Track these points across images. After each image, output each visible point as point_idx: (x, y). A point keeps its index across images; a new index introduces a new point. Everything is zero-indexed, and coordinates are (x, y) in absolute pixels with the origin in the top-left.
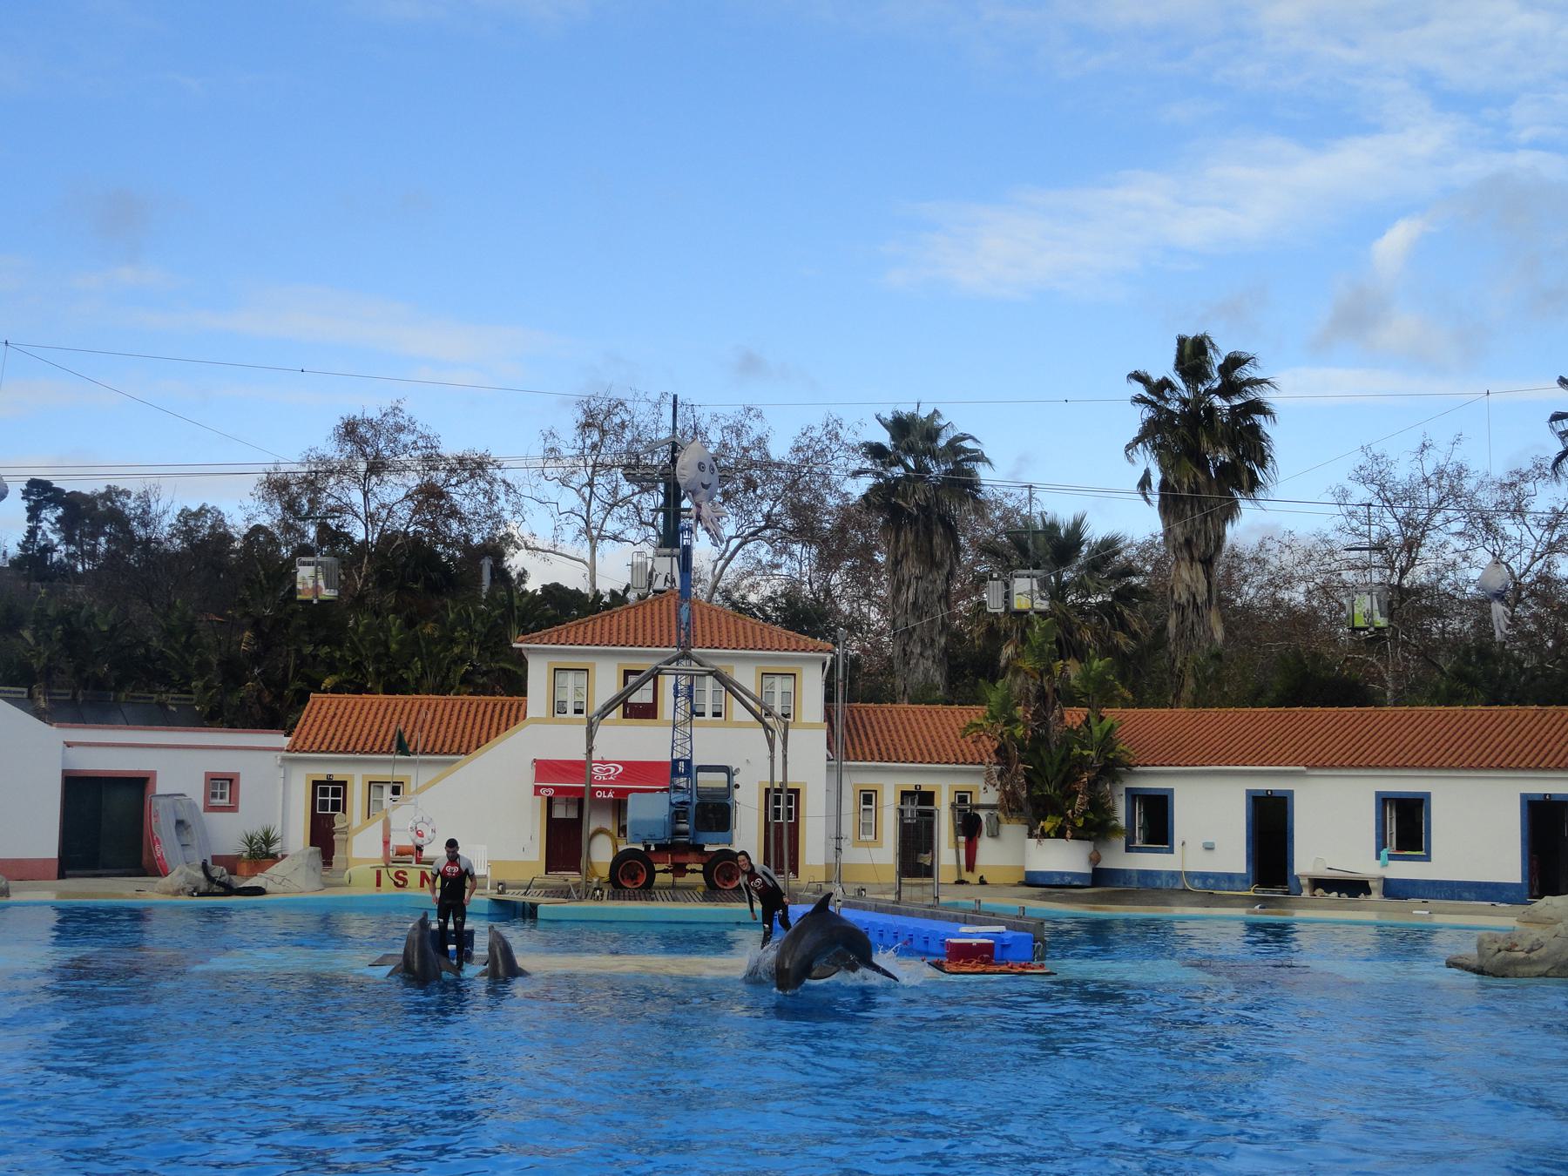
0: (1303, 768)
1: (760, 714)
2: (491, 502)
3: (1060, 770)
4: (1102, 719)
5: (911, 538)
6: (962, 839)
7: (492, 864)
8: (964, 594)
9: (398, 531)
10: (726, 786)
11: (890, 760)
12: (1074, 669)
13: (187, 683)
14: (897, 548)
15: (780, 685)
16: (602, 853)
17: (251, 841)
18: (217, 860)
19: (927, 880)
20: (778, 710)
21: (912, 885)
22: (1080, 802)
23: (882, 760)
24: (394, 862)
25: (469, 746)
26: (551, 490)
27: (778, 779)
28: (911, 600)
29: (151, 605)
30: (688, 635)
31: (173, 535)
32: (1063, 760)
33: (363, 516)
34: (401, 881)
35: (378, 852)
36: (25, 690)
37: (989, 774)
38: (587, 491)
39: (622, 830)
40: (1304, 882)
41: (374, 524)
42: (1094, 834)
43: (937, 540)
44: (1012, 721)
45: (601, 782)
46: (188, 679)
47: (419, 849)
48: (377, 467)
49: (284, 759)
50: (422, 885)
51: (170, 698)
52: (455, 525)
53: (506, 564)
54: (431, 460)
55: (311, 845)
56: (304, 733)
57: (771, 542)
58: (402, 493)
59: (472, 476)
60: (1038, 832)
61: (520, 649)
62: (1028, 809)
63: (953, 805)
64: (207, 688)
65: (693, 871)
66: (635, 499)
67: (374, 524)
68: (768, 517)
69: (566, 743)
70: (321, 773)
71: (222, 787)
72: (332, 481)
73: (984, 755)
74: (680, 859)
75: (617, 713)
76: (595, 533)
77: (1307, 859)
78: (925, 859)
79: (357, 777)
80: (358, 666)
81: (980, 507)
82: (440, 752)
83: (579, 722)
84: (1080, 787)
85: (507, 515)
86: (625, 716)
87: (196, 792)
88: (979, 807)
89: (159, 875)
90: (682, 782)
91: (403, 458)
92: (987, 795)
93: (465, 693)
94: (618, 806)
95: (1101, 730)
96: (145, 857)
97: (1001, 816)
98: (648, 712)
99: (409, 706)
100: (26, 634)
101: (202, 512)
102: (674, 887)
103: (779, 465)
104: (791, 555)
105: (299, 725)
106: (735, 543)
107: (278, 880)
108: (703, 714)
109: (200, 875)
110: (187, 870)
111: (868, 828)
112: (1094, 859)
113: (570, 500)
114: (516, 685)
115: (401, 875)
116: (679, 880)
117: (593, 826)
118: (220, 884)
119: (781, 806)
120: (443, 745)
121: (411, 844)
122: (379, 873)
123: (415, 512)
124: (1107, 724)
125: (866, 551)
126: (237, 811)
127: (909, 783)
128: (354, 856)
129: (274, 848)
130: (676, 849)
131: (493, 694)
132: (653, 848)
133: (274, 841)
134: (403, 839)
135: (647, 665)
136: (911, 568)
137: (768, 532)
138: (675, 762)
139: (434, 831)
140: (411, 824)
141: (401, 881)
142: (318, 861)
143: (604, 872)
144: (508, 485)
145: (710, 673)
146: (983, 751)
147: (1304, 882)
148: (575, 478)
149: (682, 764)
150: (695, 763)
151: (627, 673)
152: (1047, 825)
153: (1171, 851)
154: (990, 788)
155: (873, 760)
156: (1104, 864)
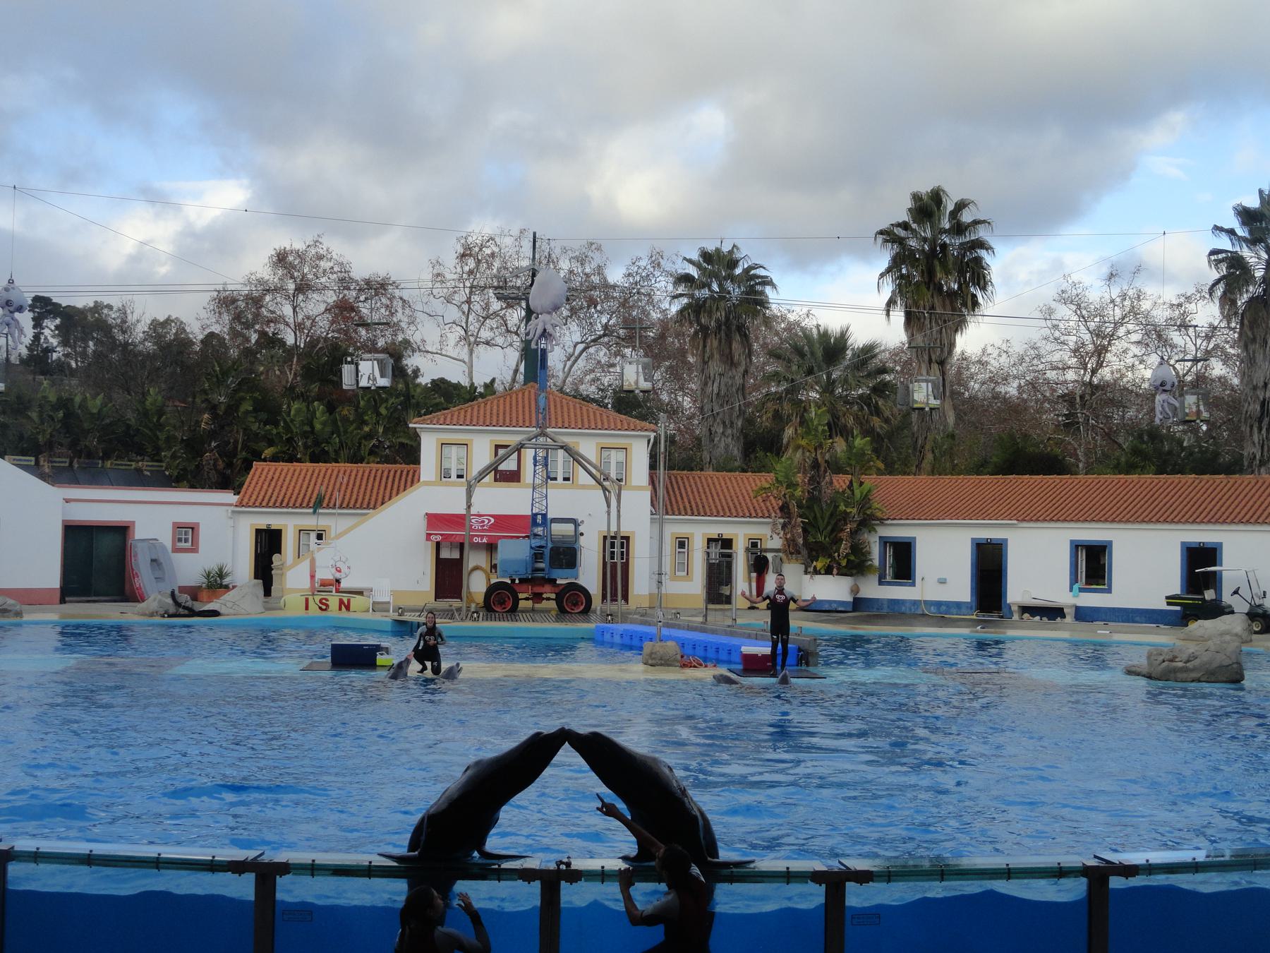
0: (1015, 522)
1: (601, 480)
2: (392, 314)
3: (828, 523)
4: (861, 484)
5: (715, 343)
6: (754, 575)
7: (394, 593)
8: (756, 388)
9: (320, 337)
10: (573, 534)
11: (699, 514)
12: (840, 445)
13: (158, 454)
14: (704, 351)
15: (615, 457)
16: (477, 585)
17: (208, 576)
18: (183, 589)
19: (727, 606)
20: (613, 475)
21: (716, 610)
22: (844, 548)
23: (693, 514)
24: (319, 591)
25: (376, 503)
26: (437, 306)
27: (614, 528)
28: (716, 391)
29: (129, 394)
30: (544, 419)
31: (145, 340)
32: (832, 515)
33: (292, 326)
34: (324, 606)
35: (306, 584)
36: (33, 458)
37: (775, 524)
38: (465, 307)
39: (494, 567)
41: (301, 330)
42: (854, 571)
43: (735, 345)
44: (791, 485)
45: (478, 531)
46: (158, 450)
47: (338, 581)
48: (303, 287)
49: (233, 512)
50: (340, 609)
51: (145, 465)
52: (363, 332)
53: (405, 362)
54: (345, 283)
55: (256, 577)
56: (249, 492)
57: (607, 345)
58: (322, 308)
59: (376, 295)
60: (811, 569)
61: (415, 428)
62: (805, 552)
63: (747, 549)
64: (174, 457)
65: (548, 599)
66: (503, 312)
67: (301, 330)
68: (606, 327)
69: (450, 501)
70: (263, 522)
71: (187, 534)
72: (268, 298)
73: (772, 511)
74: (538, 590)
75: (489, 478)
76: (472, 339)
77: (1017, 591)
78: (725, 590)
79: (289, 524)
80: (290, 441)
81: (768, 321)
82: (354, 507)
83: (461, 485)
84: (844, 535)
85: (403, 325)
86: (496, 480)
87: (166, 539)
88: (767, 550)
89: (138, 601)
90: (539, 530)
91: (323, 280)
92: (776, 542)
93: (373, 462)
94: (491, 548)
95: (862, 493)
96: (127, 587)
97: (784, 557)
98: (513, 477)
99: (329, 471)
100: (34, 415)
101: (168, 321)
102: (533, 610)
103: (614, 287)
104: (623, 356)
105: (245, 486)
106: (581, 347)
107: (229, 605)
108: (555, 479)
109: (170, 601)
110: (159, 597)
112: (855, 590)
113: (453, 313)
114: (411, 454)
115: (324, 601)
116: (537, 606)
117: (471, 566)
118: (185, 608)
119: (615, 550)
120: (356, 502)
121: (331, 577)
122: (307, 600)
123: (332, 322)
124: (866, 486)
125: (682, 353)
126: (197, 552)
127: (714, 531)
128: (288, 587)
129: (226, 581)
130: (535, 581)
131: (395, 462)
132: (517, 581)
133: (227, 575)
134: (325, 574)
135: (512, 440)
136: (715, 367)
137: (606, 339)
138: (535, 515)
139: (349, 568)
140: (332, 562)
141: (324, 606)
142: (261, 591)
143: (480, 599)
144: (404, 301)
145: (562, 447)
146: (770, 508)
147: (1015, 608)
148: (456, 297)
149: (539, 517)
150: (550, 516)
151: (497, 447)
152: (819, 564)
153: (913, 585)
154: (775, 536)
155: (686, 514)
156: (859, 596)
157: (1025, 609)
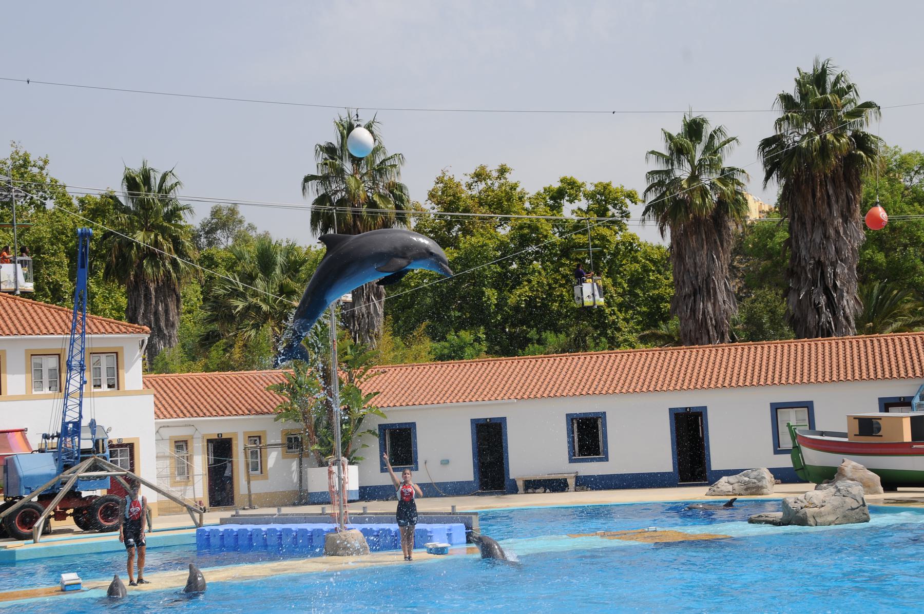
40: (520, 484)
111: (184, 471)
147: (520, 484)
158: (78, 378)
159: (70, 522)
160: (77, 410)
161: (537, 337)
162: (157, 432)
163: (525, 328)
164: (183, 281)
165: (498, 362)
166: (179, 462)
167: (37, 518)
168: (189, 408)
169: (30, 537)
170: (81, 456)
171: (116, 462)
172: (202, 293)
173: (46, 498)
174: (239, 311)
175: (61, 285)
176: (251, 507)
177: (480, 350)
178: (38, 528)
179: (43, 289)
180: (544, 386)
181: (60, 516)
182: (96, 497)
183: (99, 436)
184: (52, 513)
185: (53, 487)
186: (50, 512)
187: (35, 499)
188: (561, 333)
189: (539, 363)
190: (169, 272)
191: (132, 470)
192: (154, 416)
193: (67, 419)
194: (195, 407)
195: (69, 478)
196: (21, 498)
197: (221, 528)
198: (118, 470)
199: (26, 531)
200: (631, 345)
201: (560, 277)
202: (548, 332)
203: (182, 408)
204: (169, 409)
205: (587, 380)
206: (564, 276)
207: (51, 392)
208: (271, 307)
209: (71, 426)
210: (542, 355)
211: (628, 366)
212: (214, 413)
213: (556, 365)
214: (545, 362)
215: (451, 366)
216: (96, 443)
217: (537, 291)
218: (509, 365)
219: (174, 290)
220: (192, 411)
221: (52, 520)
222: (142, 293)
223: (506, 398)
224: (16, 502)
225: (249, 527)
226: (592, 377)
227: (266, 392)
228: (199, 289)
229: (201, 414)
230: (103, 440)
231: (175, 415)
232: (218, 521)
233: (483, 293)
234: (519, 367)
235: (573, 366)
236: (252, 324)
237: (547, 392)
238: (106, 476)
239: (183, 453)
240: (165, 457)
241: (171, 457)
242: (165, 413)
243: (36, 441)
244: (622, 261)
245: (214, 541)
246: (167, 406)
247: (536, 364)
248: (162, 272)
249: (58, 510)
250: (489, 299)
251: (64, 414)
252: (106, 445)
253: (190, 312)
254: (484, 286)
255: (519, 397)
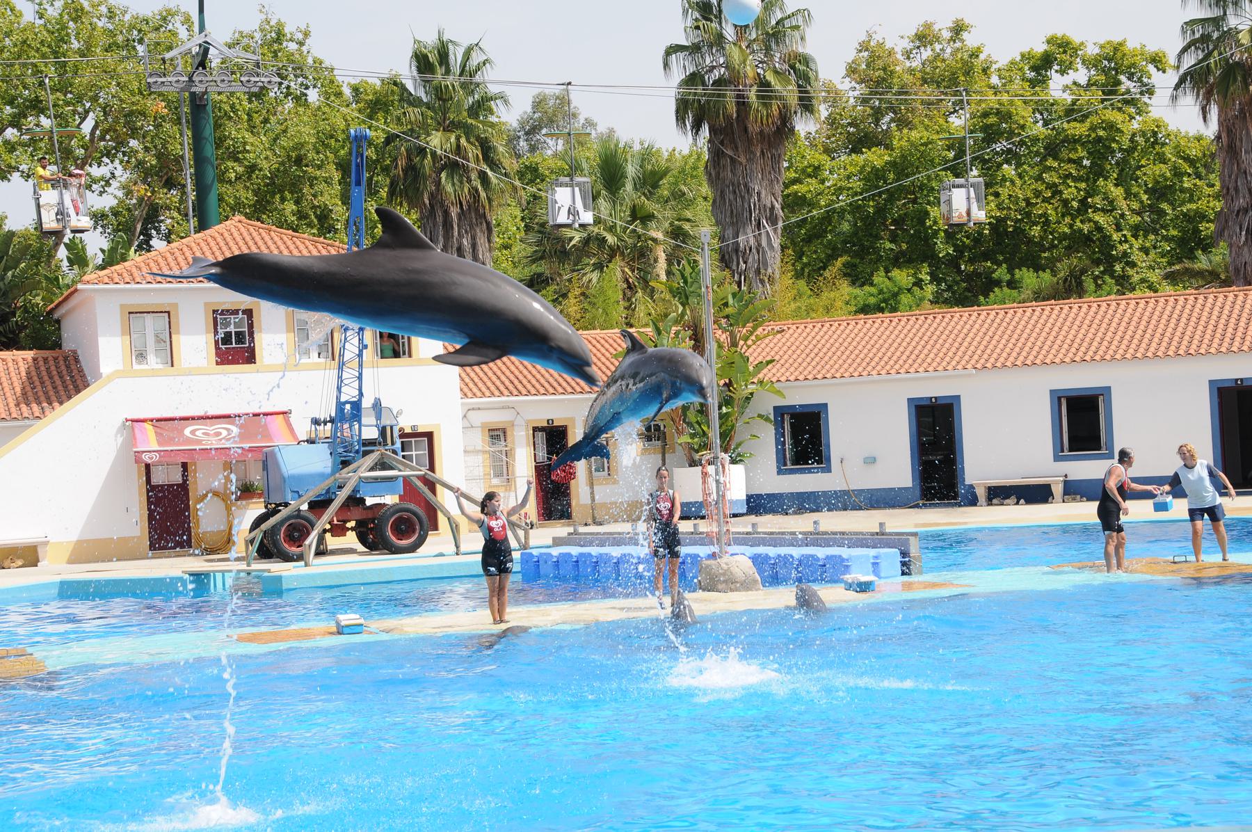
40: (981, 493)
111: (503, 469)
147: (981, 493)
153: (828, 470)
157: (998, 494)
158: (356, 341)
159: (351, 540)
160: (356, 384)
161: (1008, 277)
162: (465, 416)
163: (989, 264)
164: (495, 203)
165: (949, 316)
166: (495, 458)
167: (308, 534)
168: (507, 383)
169: (300, 558)
170: (363, 449)
171: (409, 458)
172: (523, 219)
173: (318, 506)
174: (574, 245)
175: (331, 211)
176: (596, 522)
177: (922, 299)
178: (310, 546)
179: (306, 217)
180: (1017, 349)
181: (338, 530)
182: (384, 505)
183: (386, 421)
184: (328, 527)
185: (328, 491)
186: (324, 524)
187: (305, 507)
188: (1044, 271)
189: (1009, 315)
190: (477, 190)
191: (432, 468)
192: (459, 394)
193: (343, 399)
194: (516, 382)
195: (349, 479)
196: (286, 505)
197: (556, 552)
198: (412, 469)
199: (294, 550)
200: (1151, 287)
201: (1043, 187)
202: (1024, 269)
203: (498, 383)
204: (480, 385)
205: (1083, 340)
206: (1051, 185)
207: (322, 360)
208: (620, 239)
209: (348, 407)
210: (1015, 305)
211: (1145, 318)
212: (542, 391)
213: (1035, 318)
214: (1019, 315)
215: (879, 321)
216: (383, 432)
217: (1010, 208)
218: (964, 319)
219: (484, 216)
220: (511, 387)
221: (328, 535)
222: (440, 219)
223: (960, 367)
224: (280, 511)
225: (594, 551)
226: (1090, 335)
227: (613, 360)
228: (518, 213)
229: (524, 392)
230: (392, 427)
231: (488, 393)
232: (550, 542)
233: (927, 214)
234: (979, 322)
235: (1061, 320)
236: (594, 264)
237: (1021, 358)
238: (396, 478)
239: (501, 446)
240: (477, 452)
241: (484, 452)
242: (475, 390)
243: (303, 429)
244: (1140, 161)
245: (546, 569)
246: (476, 379)
247: (1005, 317)
248: (466, 190)
249: (335, 522)
250: (935, 223)
251: (339, 389)
252: (396, 434)
253: (506, 247)
254: (929, 203)
255: (979, 366)
